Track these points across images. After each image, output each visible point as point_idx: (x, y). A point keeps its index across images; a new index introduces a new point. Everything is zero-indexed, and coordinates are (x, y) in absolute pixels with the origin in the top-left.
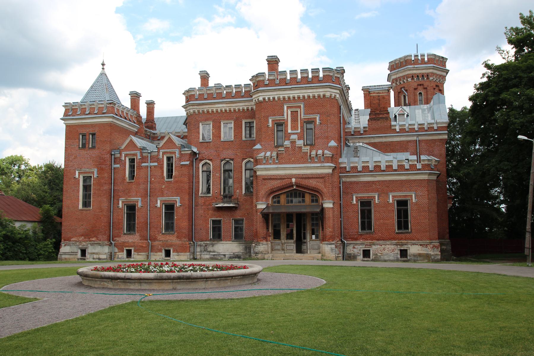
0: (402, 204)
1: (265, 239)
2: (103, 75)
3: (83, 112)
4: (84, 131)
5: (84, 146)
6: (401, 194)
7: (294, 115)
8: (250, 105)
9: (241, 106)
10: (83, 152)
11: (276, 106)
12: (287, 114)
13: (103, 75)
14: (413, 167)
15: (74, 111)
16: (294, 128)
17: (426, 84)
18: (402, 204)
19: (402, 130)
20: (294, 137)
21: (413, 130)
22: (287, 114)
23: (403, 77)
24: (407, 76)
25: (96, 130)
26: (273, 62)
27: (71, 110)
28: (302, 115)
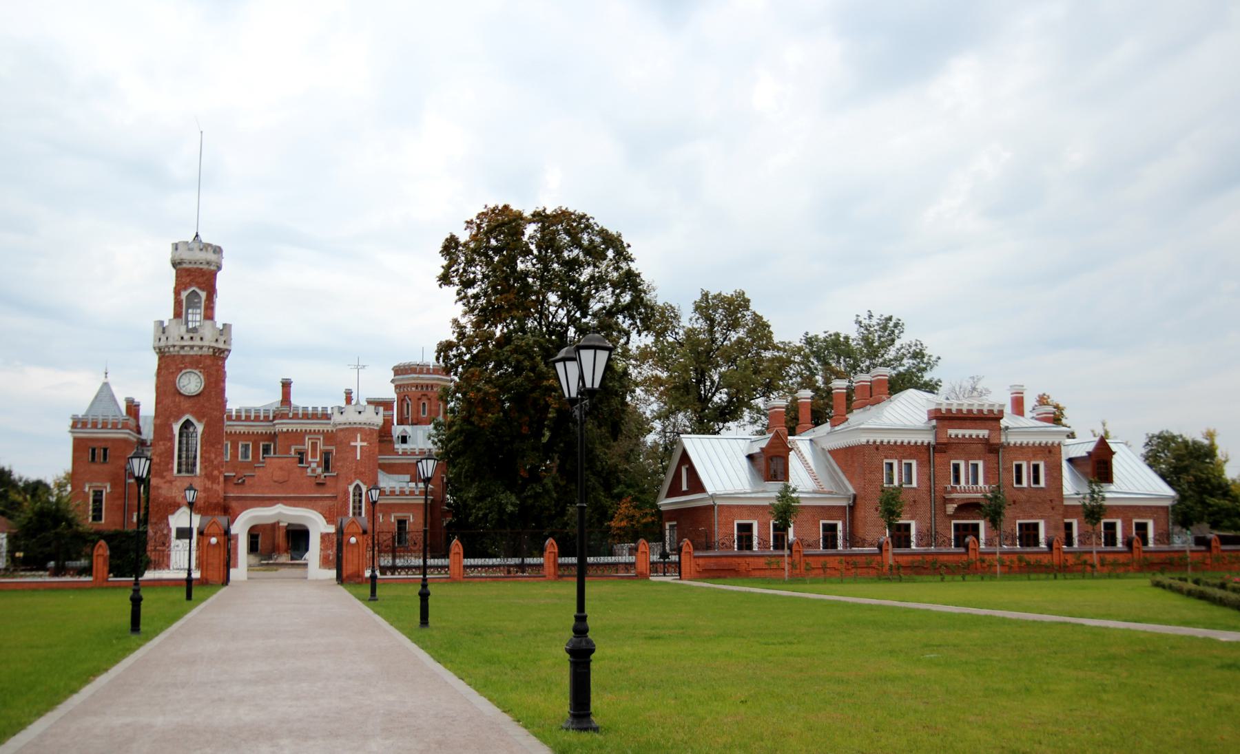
0: (402, 523)
1: (286, 551)
2: (106, 385)
3: (95, 425)
4: (95, 445)
5: (93, 458)
6: (400, 515)
7: (314, 445)
8: (271, 430)
9: (260, 428)
10: (95, 467)
11: (298, 437)
12: (308, 445)
13: (106, 385)
14: (412, 493)
15: (85, 425)
16: (314, 456)
17: (431, 394)
18: (402, 523)
19: (404, 453)
20: (314, 465)
21: (413, 454)
22: (308, 445)
23: (408, 385)
24: (412, 385)
25: (109, 445)
26: (286, 385)
27: (77, 423)
28: (321, 446)
